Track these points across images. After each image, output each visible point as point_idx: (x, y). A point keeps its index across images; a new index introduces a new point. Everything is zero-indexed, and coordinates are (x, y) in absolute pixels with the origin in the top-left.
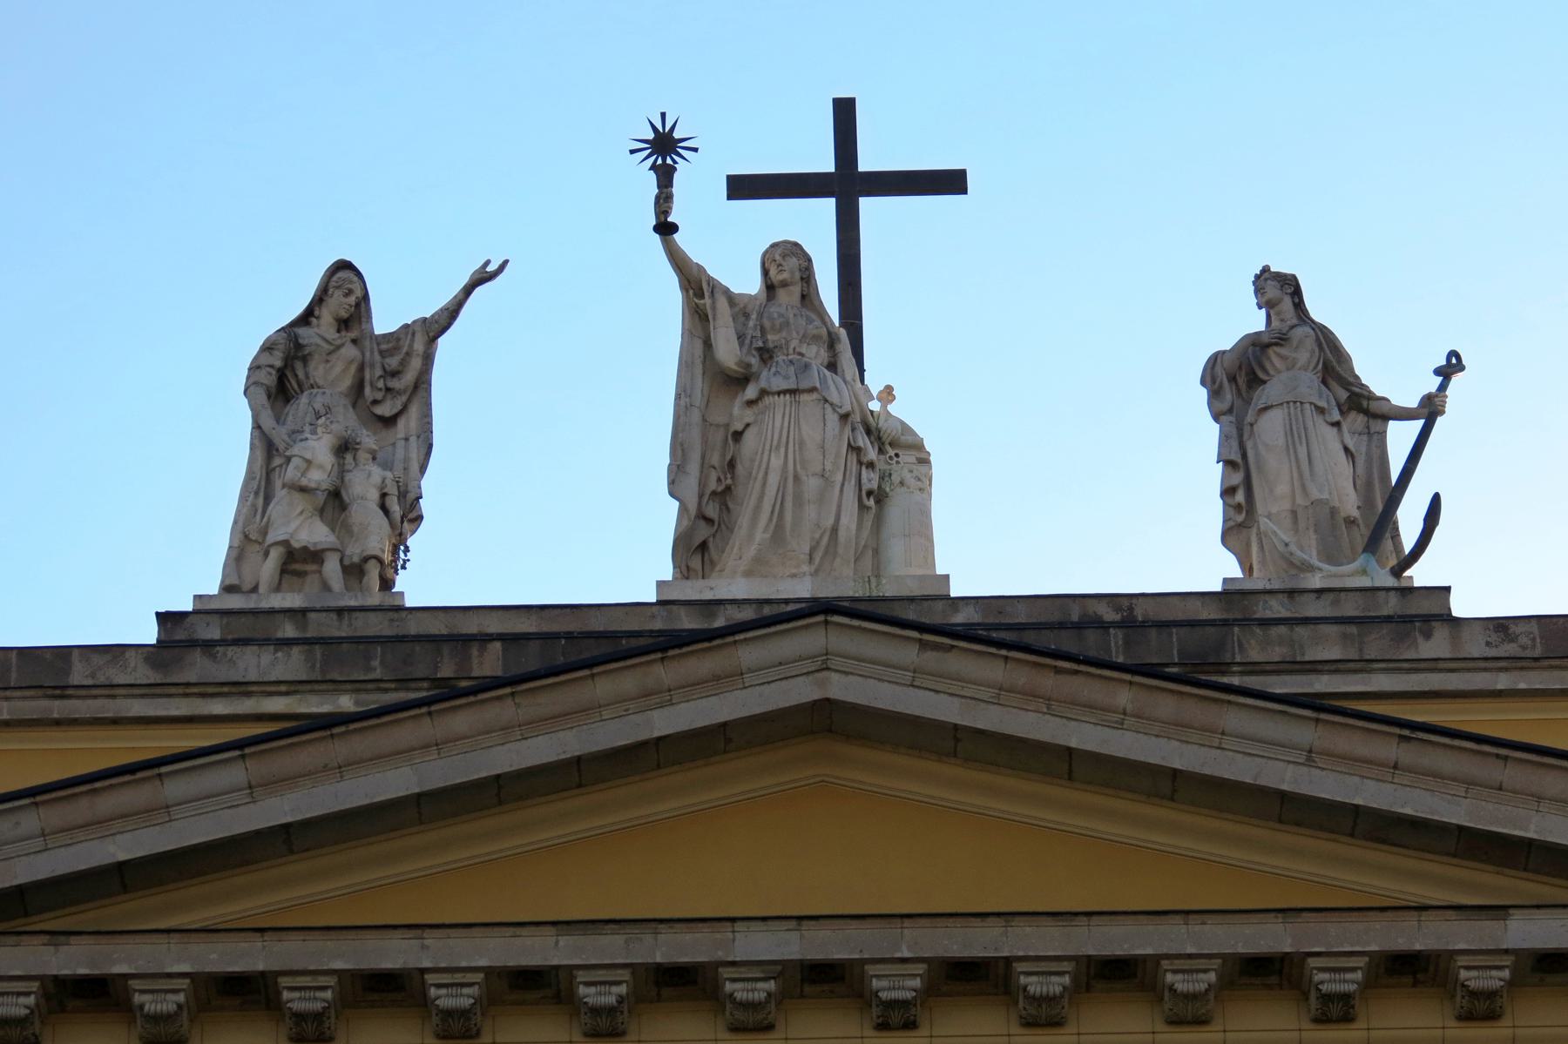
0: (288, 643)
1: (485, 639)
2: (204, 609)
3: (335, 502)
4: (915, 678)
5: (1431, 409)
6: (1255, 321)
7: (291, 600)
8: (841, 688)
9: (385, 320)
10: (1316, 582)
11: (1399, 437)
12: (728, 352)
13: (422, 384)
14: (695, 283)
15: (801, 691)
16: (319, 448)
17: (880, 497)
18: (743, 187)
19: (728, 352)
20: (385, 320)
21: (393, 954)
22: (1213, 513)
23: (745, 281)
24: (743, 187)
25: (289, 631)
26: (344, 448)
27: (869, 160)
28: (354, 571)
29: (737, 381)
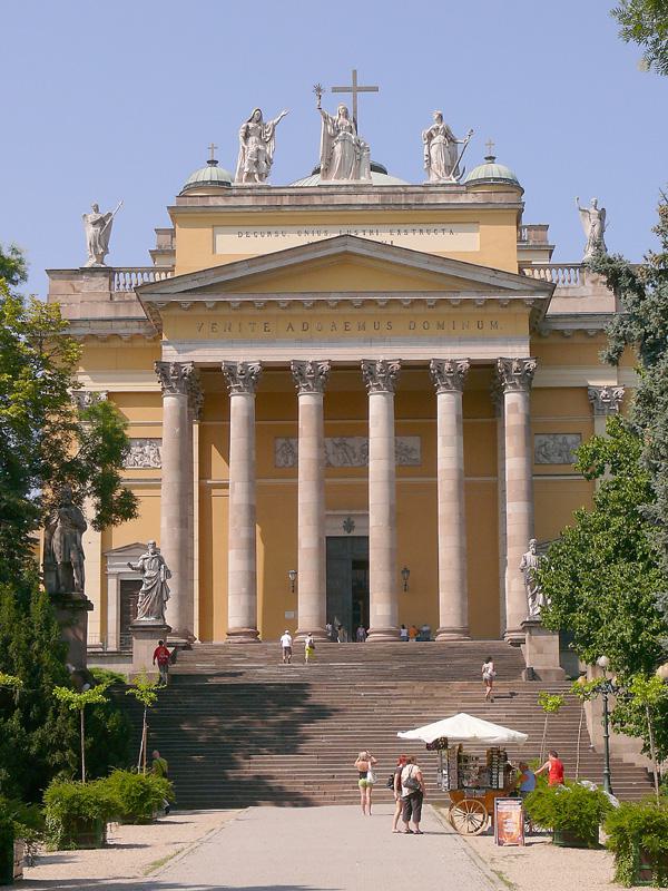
0: (248, 195)
1: (285, 195)
7: (250, 184)
8: (350, 249)
10: (441, 182)
11: (460, 148)
15: (342, 249)
17: (360, 160)
18: (335, 90)
24: (335, 90)
25: (249, 192)
28: (260, 176)
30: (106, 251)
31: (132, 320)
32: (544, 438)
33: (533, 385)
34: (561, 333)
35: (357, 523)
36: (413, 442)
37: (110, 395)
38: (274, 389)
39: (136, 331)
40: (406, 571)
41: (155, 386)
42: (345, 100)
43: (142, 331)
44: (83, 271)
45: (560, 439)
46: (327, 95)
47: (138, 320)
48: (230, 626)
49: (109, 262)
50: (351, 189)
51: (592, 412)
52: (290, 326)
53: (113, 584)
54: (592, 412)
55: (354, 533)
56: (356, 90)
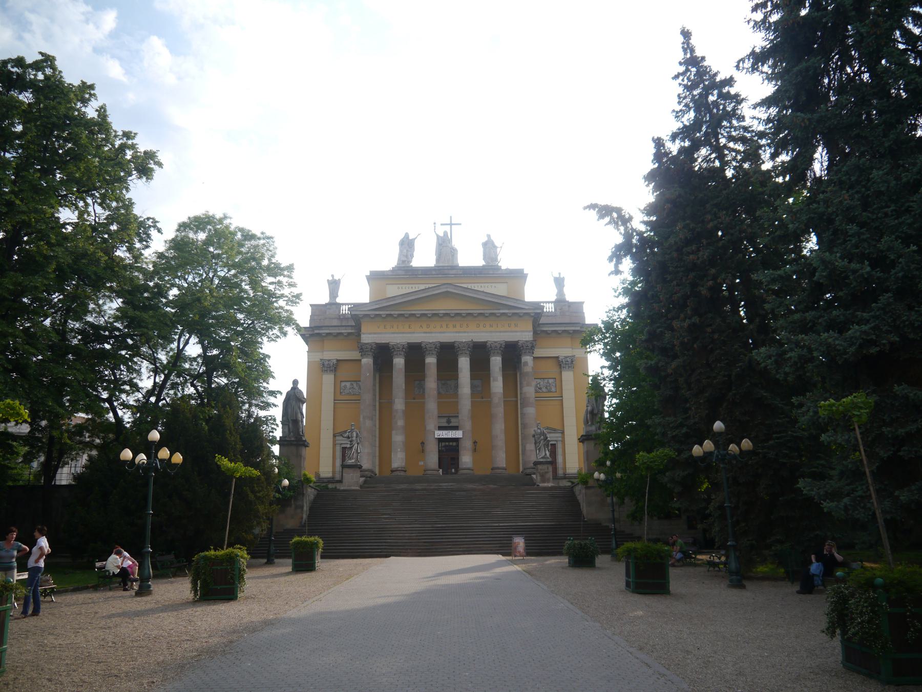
2: (396, 267)
3: (407, 256)
4: (455, 289)
5: (501, 247)
6: (486, 239)
7: (403, 265)
8: (449, 290)
9: (411, 238)
11: (498, 250)
12: (440, 242)
13: (414, 245)
14: (438, 236)
15: (445, 290)
16: (405, 251)
18: (442, 225)
19: (440, 242)
20: (411, 238)
21: (413, 312)
22: (482, 257)
23: (441, 234)
24: (442, 225)
25: (403, 269)
26: (407, 251)
27: (453, 222)
29: (442, 244)
30: (337, 296)
31: (348, 326)
32: (539, 381)
33: (534, 355)
34: (546, 332)
35: (453, 420)
36: (477, 382)
37: (338, 361)
38: (415, 353)
39: (350, 331)
40: (475, 442)
41: (355, 355)
42: (447, 228)
43: (353, 331)
44: (326, 304)
45: (546, 381)
46: (438, 225)
47: (351, 326)
48: (393, 467)
49: (339, 300)
50: (449, 268)
51: (561, 368)
52: (421, 326)
53: (338, 449)
54: (561, 368)
55: (451, 425)
56: (451, 224)
